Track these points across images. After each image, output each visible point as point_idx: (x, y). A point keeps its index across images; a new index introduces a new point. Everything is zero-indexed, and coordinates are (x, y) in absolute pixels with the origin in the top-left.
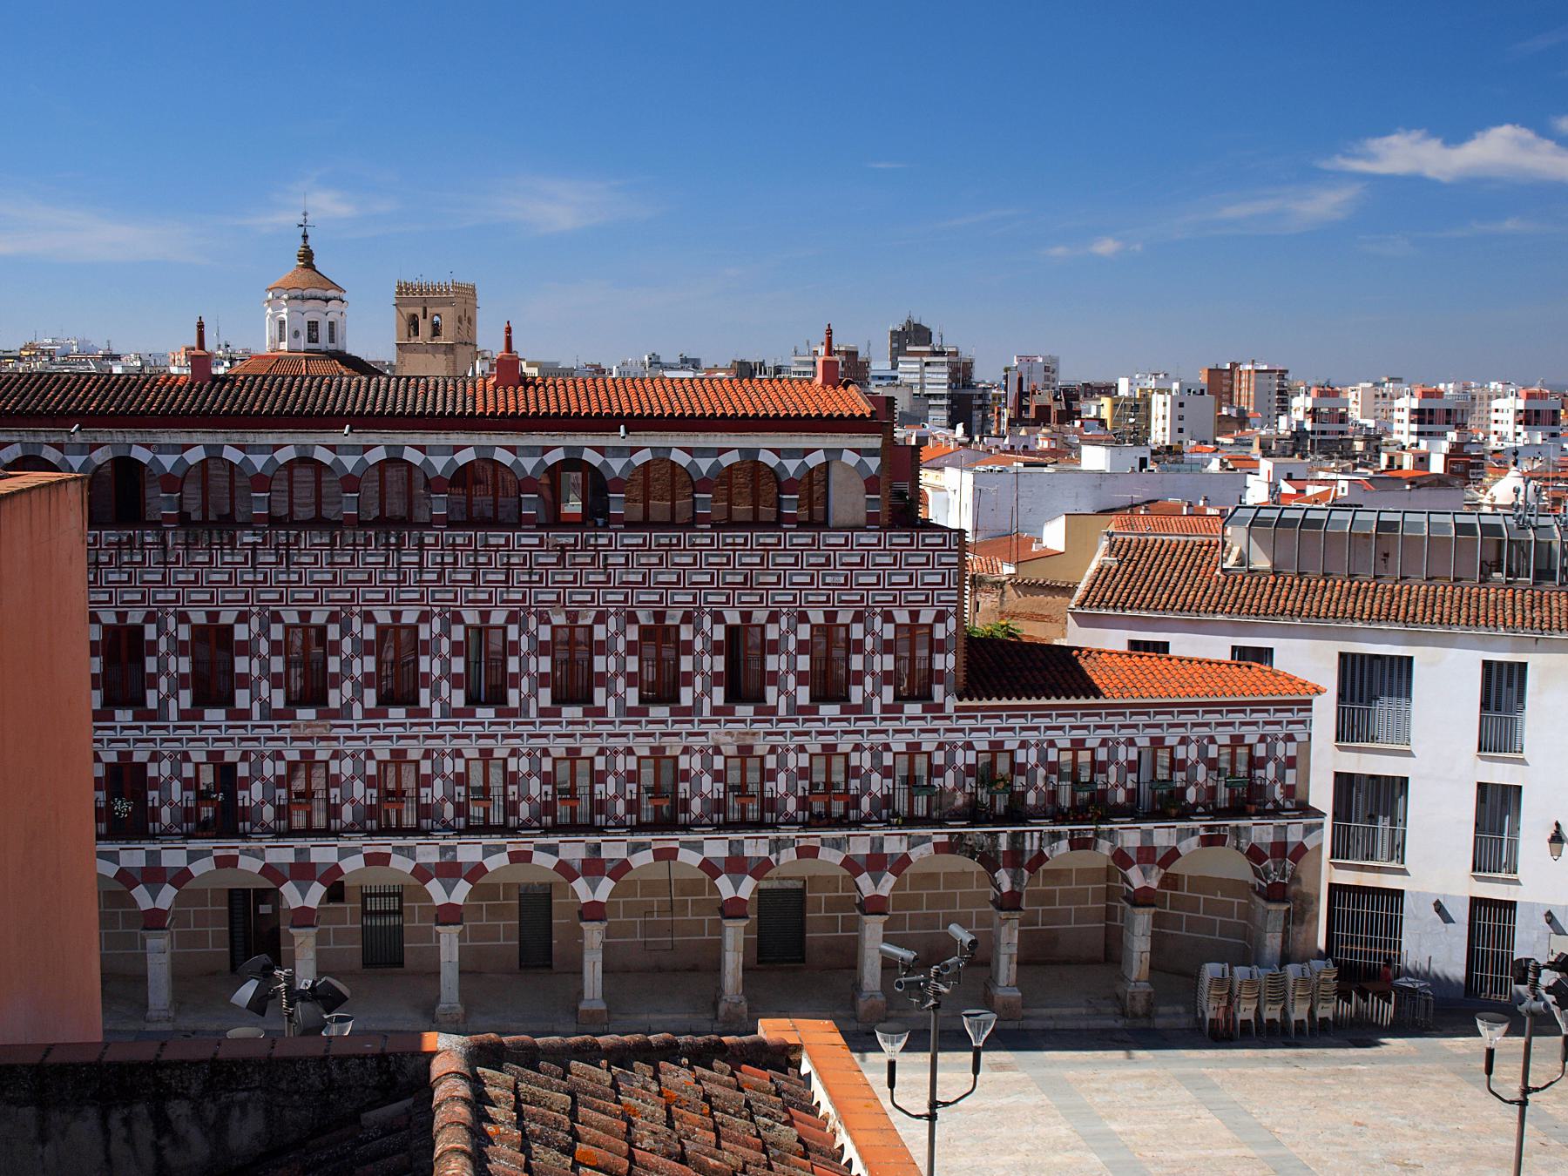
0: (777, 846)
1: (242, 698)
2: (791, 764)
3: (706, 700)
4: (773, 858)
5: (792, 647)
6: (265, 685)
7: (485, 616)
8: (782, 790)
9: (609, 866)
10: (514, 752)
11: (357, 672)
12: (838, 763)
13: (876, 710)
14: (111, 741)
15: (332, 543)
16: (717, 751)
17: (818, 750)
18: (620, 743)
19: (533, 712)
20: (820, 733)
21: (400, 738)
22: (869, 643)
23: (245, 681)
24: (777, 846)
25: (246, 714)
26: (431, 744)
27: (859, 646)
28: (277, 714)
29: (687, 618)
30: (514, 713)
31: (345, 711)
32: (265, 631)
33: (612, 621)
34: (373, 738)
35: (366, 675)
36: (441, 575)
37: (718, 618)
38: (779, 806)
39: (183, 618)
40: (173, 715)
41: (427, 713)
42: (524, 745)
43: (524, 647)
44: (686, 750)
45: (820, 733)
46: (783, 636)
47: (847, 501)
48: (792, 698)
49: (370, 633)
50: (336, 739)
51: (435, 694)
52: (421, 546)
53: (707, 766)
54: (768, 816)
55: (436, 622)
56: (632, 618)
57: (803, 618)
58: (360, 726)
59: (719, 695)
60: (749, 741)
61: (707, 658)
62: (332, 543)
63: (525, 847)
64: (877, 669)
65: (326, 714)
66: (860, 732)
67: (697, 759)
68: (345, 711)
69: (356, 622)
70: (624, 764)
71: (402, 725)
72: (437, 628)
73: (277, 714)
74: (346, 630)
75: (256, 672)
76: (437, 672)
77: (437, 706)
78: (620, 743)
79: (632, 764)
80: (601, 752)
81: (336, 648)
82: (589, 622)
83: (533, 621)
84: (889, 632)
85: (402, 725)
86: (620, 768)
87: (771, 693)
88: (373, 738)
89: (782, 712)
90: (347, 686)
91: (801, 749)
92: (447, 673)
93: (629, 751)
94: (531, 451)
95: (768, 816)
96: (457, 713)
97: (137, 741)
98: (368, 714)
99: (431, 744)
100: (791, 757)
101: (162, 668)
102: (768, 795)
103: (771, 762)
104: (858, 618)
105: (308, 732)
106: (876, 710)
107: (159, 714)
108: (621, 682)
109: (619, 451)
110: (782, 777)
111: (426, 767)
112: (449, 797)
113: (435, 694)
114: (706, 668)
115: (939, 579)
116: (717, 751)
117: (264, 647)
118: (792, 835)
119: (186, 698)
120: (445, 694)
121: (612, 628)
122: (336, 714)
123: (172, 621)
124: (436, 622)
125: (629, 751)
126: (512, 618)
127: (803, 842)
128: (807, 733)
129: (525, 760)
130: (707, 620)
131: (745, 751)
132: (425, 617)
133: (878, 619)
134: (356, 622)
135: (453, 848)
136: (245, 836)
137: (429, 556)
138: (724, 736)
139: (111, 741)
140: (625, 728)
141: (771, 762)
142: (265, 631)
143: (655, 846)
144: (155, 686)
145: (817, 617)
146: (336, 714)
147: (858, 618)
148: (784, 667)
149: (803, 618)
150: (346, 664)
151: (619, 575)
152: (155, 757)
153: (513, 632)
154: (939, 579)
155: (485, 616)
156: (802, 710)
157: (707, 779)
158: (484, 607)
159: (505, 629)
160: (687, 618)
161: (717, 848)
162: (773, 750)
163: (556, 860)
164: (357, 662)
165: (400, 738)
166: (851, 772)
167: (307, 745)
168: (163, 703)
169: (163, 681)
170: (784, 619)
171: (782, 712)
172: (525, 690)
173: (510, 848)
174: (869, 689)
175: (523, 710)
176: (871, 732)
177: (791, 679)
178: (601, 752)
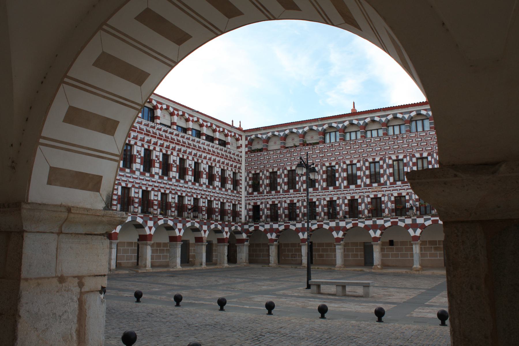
1: (359, 182)
6: (364, 178)
7: (421, 155)
14: (328, 195)
21: (400, 190)
23: (360, 177)
25: (360, 186)
31: (385, 183)
34: (393, 190)
35: (390, 173)
39: (344, 163)
40: (342, 187)
50: (383, 191)
55: (408, 157)
58: (389, 187)
68: (385, 183)
71: (401, 186)
74: (384, 162)
75: (362, 175)
81: (381, 167)
85: (401, 186)
88: (393, 190)
90: (385, 177)
97: (334, 194)
98: (391, 184)
101: (340, 175)
105: (376, 190)
107: (339, 187)
117: (364, 168)
119: (345, 183)
122: (383, 184)
123: (342, 164)
124: (408, 157)
126: (429, 154)
132: (405, 157)
136: (360, 218)
139: (328, 195)
144: (338, 180)
150: (385, 171)
152: (339, 198)
155: (421, 155)
158: (421, 152)
164: (387, 170)
165: (400, 190)
167: (375, 193)
168: (340, 184)
169: (340, 179)
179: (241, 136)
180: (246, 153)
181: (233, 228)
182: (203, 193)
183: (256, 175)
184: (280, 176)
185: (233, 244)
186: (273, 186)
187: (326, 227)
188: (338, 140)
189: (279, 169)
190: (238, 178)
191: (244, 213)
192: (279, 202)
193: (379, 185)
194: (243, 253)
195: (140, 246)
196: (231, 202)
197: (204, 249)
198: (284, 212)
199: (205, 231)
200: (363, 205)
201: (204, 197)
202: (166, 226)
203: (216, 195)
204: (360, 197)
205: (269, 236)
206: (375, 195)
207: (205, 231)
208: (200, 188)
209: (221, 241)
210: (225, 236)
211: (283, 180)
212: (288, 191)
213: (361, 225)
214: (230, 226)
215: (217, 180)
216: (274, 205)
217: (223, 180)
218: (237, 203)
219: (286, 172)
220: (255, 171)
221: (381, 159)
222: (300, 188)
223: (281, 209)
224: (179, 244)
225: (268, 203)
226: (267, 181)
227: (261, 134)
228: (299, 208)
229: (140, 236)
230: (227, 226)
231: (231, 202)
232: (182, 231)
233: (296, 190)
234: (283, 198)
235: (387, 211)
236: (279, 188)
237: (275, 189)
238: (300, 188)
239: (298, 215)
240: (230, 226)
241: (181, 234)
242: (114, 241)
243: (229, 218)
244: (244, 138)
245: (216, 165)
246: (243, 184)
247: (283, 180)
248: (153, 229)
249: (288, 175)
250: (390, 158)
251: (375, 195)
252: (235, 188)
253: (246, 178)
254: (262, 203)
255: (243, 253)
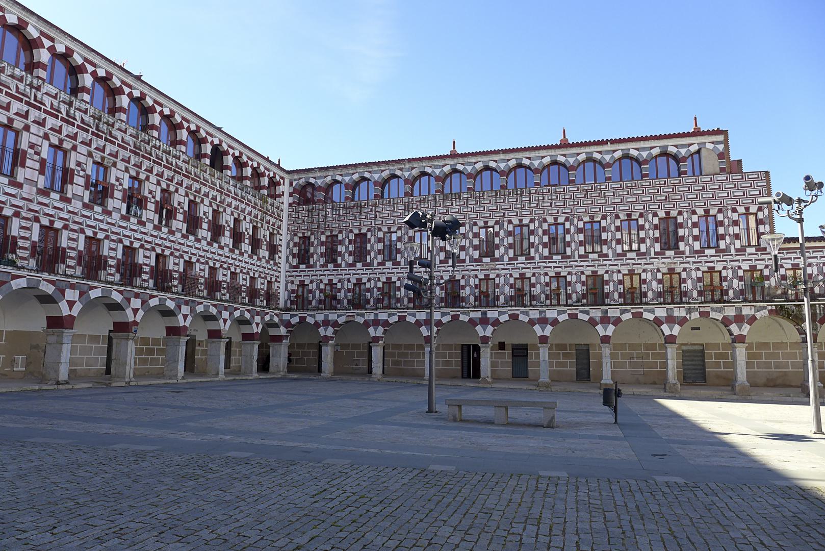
0: (689, 311)
2: (694, 275)
3: (652, 249)
4: (688, 317)
5: (690, 225)
6: (471, 249)
7: (556, 219)
8: (690, 287)
9: (612, 320)
10: (569, 273)
11: (506, 243)
12: (716, 275)
13: (733, 251)
15: (496, 195)
16: (659, 271)
17: (706, 269)
18: (615, 268)
19: (577, 257)
20: (706, 262)
22: (726, 222)
24: (689, 311)
26: (535, 270)
27: (721, 223)
28: (476, 261)
29: (641, 215)
30: (569, 257)
31: (501, 259)
32: (471, 229)
33: (609, 218)
36: (538, 204)
37: (655, 215)
38: (689, 294)
41: (533, 258)
42: (573, 270)
43: (572, 230)
44: (644, 271)
45: (706, 262)
46: (686, 220)
47: (710, 163)
48: (691, 247)
49: (511, 228)
51: (537, 251)
52: (530, 194)
53: (654, 278)
54: (684, 299)
55: (536, 222)
56: (617, 217)
57: (694, 212)
59: (658, 247)
60: (673, 266)
61: (651, 232)
62: (496, 195)
63: (575, 311)
64: (731, 233)
65: (494, 260)
66: (726, 261)
67: (649, 274)
68: (501, 259)
69: (505, 224)
70: (617, 277)
72: (537, 225)
73: (476, 261)
74: (501, 227)
75: (468, 245)
76: (537, 242)
77: (537, 255)
78: (615, 268)
79: (620, 277)
80: (607, 272)
82: (599, 219)
83: (575, 220)
84: (656, 221)
86: (615, 279)
87: (682, 245)
89: (687, 253)
90: (502, 248)
91: (698, 269)
92: (541, 242)
93: (619, 272)
94: (572, 155)
95: (684, 299)
96: (546, 258)
99: (535, 270)
100: (693, 273)
102: (683, 289)
103: (684, 275)
104: (720, 211)
105: (487, 267)
106: (733, 251)
108: (614, 243)
109: (608, 152)
110: (689, 282)
111: (533, 280)
112: (543, 292)
113: (537, 251)
114: (651, 235)
115: (757, 193)
116: (659, 271)
117: (471, 235)
118: (697, 305)
120: (540, 250)
121: (609, 221)
122: (498, 260)
124: (536, 222)
125: (619, 272)
126: (567, 219)
127: (702, 309)
128: (700, 262)
129: (574, 276)
130: (650, 216)
131: (671, 271)
132: (532, 221)
133: (730, 212)
134: (505, 224)
135: (545, 312)
137: (533, 197)
138: (663, 264)
140: (616, 262)
141: (684, 275)
142: (471, 229)
143: (632, 311)
145: (701, 212)
146: (498, 260)
147: (720, 211)
148: (687, 234)
149: (694, 212)
150: (502, 240)
151: (611, 200)
153: (567, 225)
154: (757, 193)
155: (556, 219)
156: (697, 252)
157: (654, 283)
158: (555, 216)
159: (564, 224)
160: (641, 215)
161: (661, 312)
162: (684, 270)
163: (588, 317)
164: (506, 239)
166: (722, 279)
167: (487, 272)
170: (685, 214)
171: (687, 253)
172: (573, 248)
173: (569, 312)
174: (728, 242)
175: (573, 255)
176: (731, 261)
177: (691, 239)
178: (607, 272)
179: (283, 178)
180: (290, 205)
181: (267, 318)
182: (224, 259)
183: (306, 239)
184: (341, 243)
185: (266, 340)
186: (331, 255)
187: (410, 319)
188: (433, 192)
189: (341, 232)
190: (277, 242)
191: (283, 296)
192: (340, 281)
193: (491, 261)
194: (279, 356)
195: (115, 341)
196: (265, 278)
197: (223, 347)
198: (346, 296)
199: (225, 321)
200: (468, 289)
201: (225, 266)
202: (162, 308)
203: (244, 265)
204: (463, 277)
205: (322, 331)
206: (485, 275)
207: (225, 321)
208: (220, 252)
209: (247, 337)
210: (256, 329)
211: (347, 248)
212: (353, 265)
213: (463, 318)
214: (262, 314)
215: (247, 241)
216: (330, 283)
217: (255, 244)
218: (273, 280)
219: (352, 236)
220: (304, 234)
221: (497, 223)
222: (372, 261)
223: (343, 291)
224: (184, 339)
225: (321, 282)
226: (323, 249)
227: (314, 178)
228: (368, 290)
229: (115, 323)
230: (258, 314)
231: (265, 278)
232: (189, 319)
233: (366, 264)
234: (346, 275)
235: (502, 299)
236: (339, 259)
237: (334, 261)
238: (372, 261)
239: (368, 302)
240: (262, 314)
241: (187, 324)
242: (66, 331)
243: (261, 301)
244: (287, 182)
245: (245, 218)
246: (284, 252)
247: (347, 248)
248: (141, 313)
249: (355, 241)
250: (510, 222)
251: (485, 275)
252: (271, 257)
253: (288, 244)
254: (312, 282)
255: (279, 356)
